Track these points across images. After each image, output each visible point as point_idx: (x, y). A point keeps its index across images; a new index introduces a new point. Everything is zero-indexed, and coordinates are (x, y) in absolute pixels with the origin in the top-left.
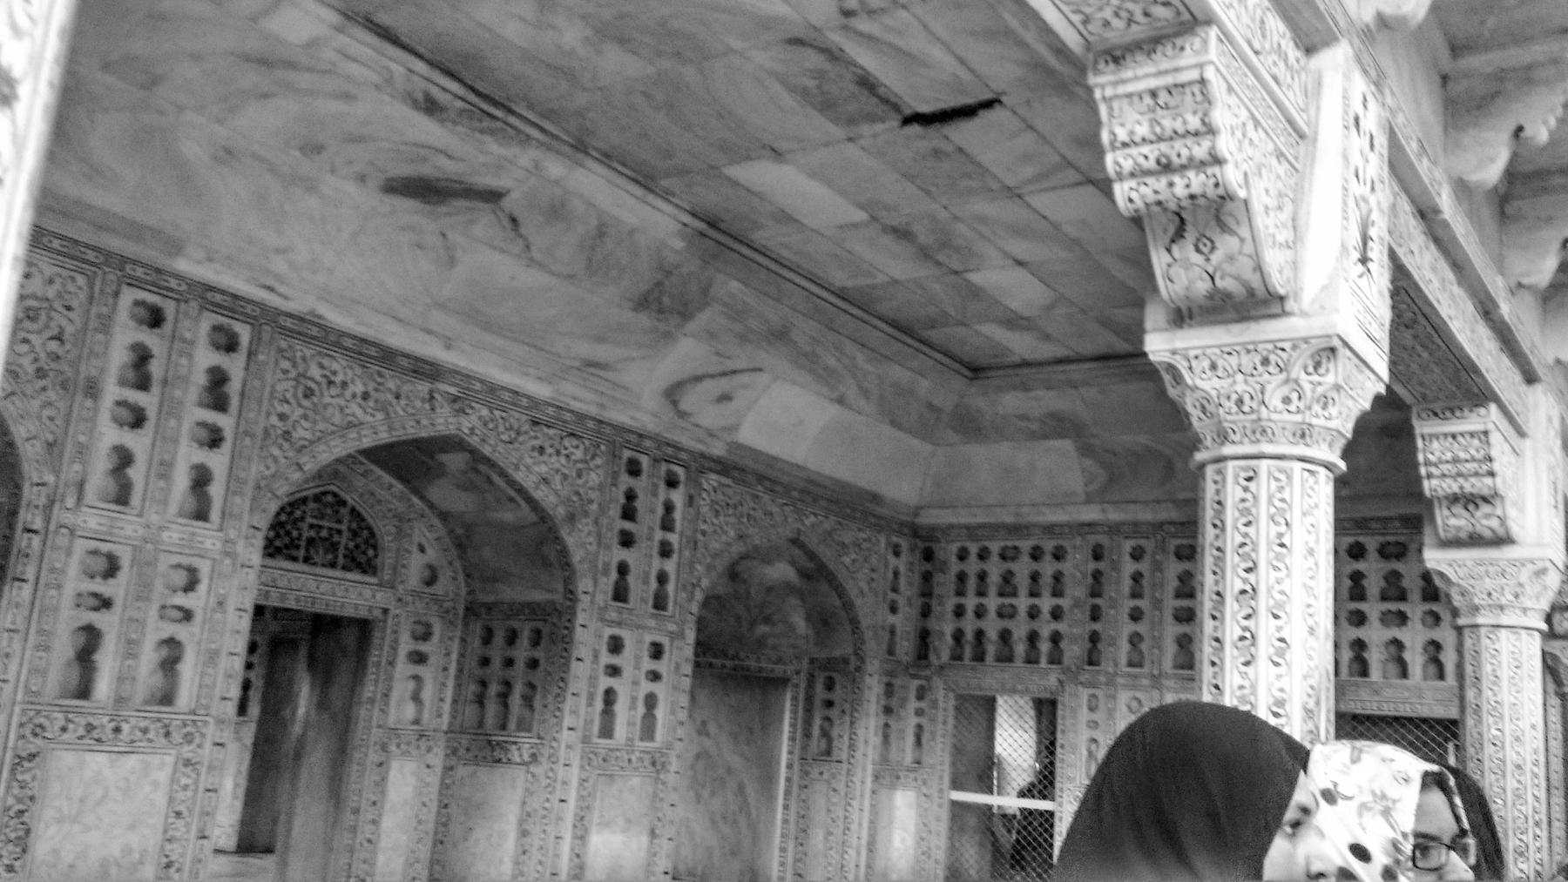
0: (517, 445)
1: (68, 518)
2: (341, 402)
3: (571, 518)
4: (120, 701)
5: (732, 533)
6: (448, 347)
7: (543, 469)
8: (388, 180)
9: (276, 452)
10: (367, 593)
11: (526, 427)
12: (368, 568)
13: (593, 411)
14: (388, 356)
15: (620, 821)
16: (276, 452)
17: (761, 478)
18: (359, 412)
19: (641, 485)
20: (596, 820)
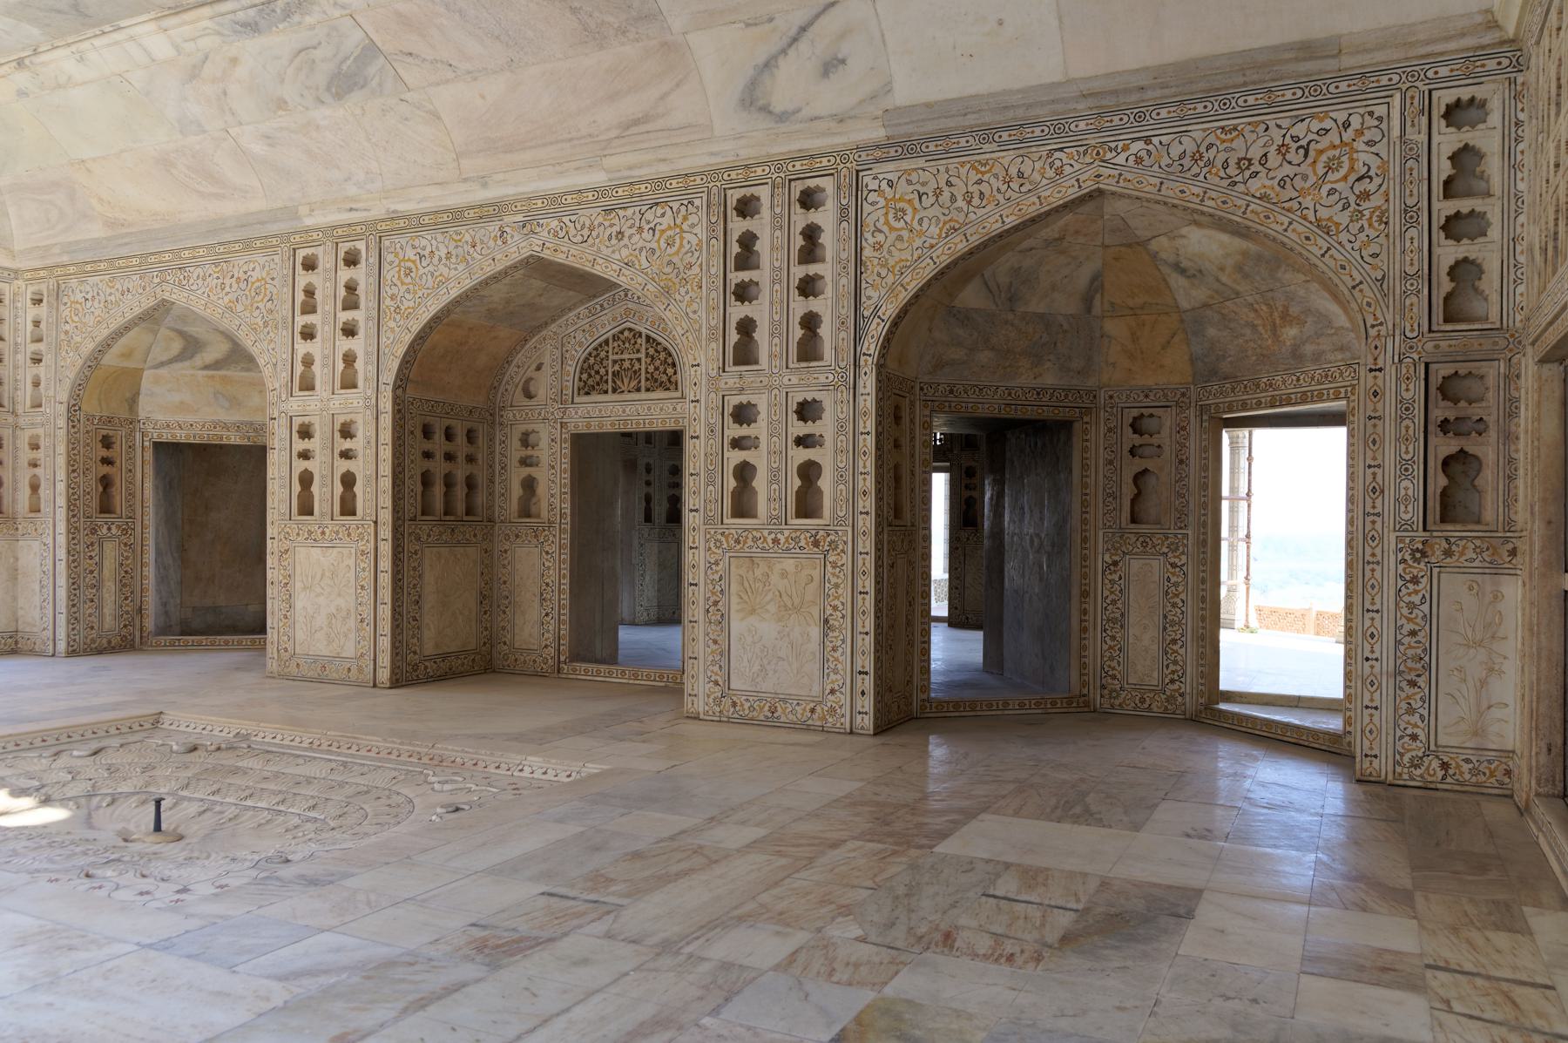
0: (590, 241)
1: (284, 407)
2: (431, 268)
3: (667, 292)
4: (322, 514)
5: (934, 230)
6: (485, 185)
7: (625, 252)
8: (328, 89)
9: (392, 324)
10: (668, 406)
11: (600, 219)
12: (670, 384)
13: (664, 169)
14: (457, 216)
15: (772, 608)
16: (392, 324)
17: (987, 133)
18: (445, 271)
19: (761, 224)
20: (734, 607)
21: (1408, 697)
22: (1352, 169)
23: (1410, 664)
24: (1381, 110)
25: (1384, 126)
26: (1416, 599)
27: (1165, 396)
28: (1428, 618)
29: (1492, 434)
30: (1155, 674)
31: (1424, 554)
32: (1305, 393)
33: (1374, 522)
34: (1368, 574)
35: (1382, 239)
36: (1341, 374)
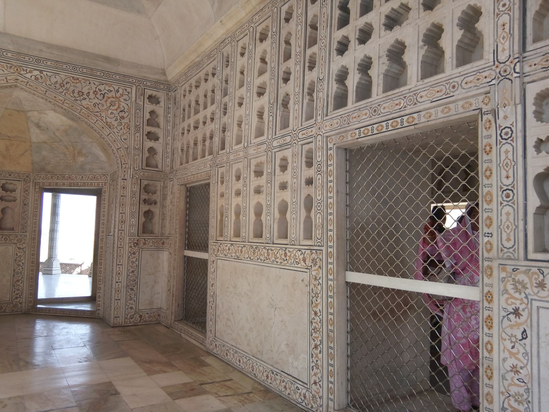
21: (130, 294)
22: (119, 107)
23: (131, 283)
24: (129, 90)
25: (130, 95)
26: (134, 260)
27: (19, 176)
28: (137, 266)
29: (158, 204)
30: (8, 296)
31: (137, 244)
32: (84, 183)
33: (121, 233)
34: (119, 251)
35: (128, 134)
36: (101, 178)
